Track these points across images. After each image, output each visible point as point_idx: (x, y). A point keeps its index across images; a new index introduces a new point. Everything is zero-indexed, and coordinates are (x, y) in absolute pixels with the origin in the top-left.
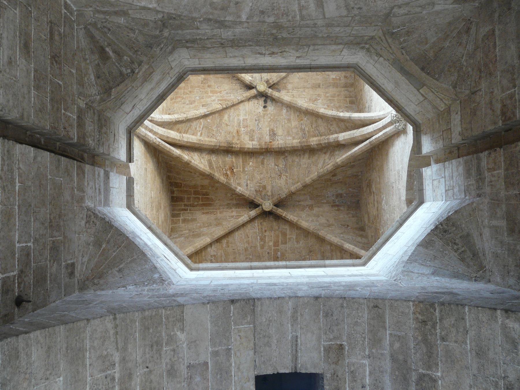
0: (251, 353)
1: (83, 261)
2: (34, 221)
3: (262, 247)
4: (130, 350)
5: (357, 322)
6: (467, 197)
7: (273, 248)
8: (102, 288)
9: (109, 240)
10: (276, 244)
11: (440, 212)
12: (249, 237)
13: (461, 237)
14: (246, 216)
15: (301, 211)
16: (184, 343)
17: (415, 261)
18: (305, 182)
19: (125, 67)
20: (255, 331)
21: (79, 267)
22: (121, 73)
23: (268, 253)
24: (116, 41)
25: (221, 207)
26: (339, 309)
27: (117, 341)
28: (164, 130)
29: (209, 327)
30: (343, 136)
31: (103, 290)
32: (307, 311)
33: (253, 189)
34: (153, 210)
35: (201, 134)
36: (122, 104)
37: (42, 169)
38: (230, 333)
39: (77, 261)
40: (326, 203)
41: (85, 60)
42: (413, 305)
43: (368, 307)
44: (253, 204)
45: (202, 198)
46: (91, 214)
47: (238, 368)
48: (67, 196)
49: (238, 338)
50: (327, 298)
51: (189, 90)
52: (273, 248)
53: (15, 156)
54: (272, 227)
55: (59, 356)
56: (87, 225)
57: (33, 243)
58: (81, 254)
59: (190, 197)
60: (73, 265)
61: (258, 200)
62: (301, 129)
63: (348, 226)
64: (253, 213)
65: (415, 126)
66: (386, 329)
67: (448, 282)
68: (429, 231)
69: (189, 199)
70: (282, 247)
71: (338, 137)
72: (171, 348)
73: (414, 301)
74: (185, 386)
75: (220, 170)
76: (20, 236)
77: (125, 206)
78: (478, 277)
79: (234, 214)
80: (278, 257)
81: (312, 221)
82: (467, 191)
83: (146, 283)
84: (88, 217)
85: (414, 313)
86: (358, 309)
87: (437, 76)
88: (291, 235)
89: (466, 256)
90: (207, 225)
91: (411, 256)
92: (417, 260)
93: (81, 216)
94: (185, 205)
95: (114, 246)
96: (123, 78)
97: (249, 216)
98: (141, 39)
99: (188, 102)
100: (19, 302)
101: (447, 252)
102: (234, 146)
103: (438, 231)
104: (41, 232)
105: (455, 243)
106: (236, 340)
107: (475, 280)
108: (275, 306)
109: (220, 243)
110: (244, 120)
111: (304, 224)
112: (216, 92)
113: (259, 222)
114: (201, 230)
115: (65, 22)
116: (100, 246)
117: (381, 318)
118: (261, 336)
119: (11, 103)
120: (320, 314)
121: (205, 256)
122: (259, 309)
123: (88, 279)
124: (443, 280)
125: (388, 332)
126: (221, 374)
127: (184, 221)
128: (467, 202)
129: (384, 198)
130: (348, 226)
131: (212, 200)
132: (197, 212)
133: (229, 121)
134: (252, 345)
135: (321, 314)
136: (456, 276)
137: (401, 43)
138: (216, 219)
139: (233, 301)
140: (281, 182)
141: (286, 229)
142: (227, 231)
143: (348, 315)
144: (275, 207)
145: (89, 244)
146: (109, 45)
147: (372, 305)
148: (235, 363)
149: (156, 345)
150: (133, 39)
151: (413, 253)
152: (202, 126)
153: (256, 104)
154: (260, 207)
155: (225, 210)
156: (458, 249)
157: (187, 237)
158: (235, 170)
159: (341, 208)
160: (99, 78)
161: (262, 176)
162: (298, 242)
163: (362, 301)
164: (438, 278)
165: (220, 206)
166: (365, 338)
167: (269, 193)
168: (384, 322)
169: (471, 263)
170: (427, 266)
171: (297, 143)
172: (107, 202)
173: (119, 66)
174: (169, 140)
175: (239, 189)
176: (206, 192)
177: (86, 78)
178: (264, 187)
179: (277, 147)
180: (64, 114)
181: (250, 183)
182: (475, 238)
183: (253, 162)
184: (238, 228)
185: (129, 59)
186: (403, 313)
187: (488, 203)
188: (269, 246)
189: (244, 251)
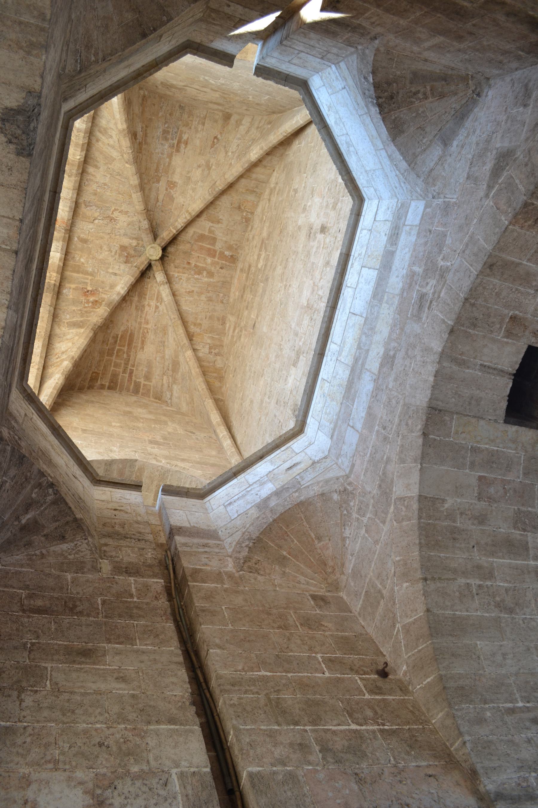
0: (482, 422)
1: (304, 582)
2: (291, 651)
3: (211, 274)
4: (456, 565)
5: (497, 292)
6: (360, 47)
7: (216, 259)
8: (340, 564)
9: (276, 545)
10: (212, 253)
11: (351, 82)
12: (193, 291)
13: (411, 83)
14: (161, 288)
15: (173, 201)
16: (456, 501)
17: (415, 156)
18: (135, 186)
19: (45, 496)
20: (462, 414)
21: (312, 588)
22: (54, 503)
23: (221, 268)
24: (13, 508)
25: (139, 320)
26: (474, 309)
27: (447, 579)
29: (446, 468)
31: (343, 565)
32: (460, 347)
33: (123, 266)
34: (138, 427)
36: (81, 499)
37: (228, 638)
38: (456, 444)
39: (306, 591)
40: (171, 160)
41: (43, 556)
42: (514, 225)
43: (488, 275)
44: (145, 273)
45: (120, 346)
46: (246, 565)
47: (493, 441)
48: (239, 600)
49: (463, 435)
50: (457, 319)
52: (216, 259)
53: (234, 676)
54: (185, 253)
55: (459, 645)
56: (262, 573)
57: (316, 653)
58: (297, 585)
59: (115, 362)
60: (314, 597)
63: (216, 138)
64: (159, 276)
65: (188, 50)
66: (521, 264)
67: (468, 135)
68: (379, 116)
69: (117, 365)
70: (218, 246)
72: (458, 516)
73: (510, 223)
74: (496, 505)
75: (86, 312)
76: (316, 670)
77: (200, 501)
78: (476, 89)
79: (153, 303)
80: (232, 256)
81: (194, 190)
82: (349, 43)
83: (345, 512)
84: (251, 570)
85: (522, 227)
86: (484, 288)
87: (165, 18)
88: (203, 226)
89: (440, 90)
90: (162, 348)
91: (404, 158)
92: (414, 154)
93: (253, 581)
94: (124, 372)
95: (285, 540)
96: (60, 501)
97: (164, 284)
98: (13, 472)
100: (384, 674)
101: (421, 110)
102: (53, 282)
103: (386, 106)
104: (299, 642)
105: (415, 94)
106: (464, 439)
107: (479, 95)
108: (443, 383)
109: (193, 336)
111: (197, 206)
113: (173, 269)
114: (167, 357)
115: (6, 586)
116: (285, 558)
117: (506, 265)
118: (468, 407)
119: (174, 680)
120: (470, 333)
121: (209, 362)
122: (440, 403)
123: (326, 579)
124: (461, 137)
125: (525, 263)
126: (493, 463)
127: (148, 377)
128: (370, 55)
129: (207, 78)
130: (216, 138)
131: (126, 331)
132: (138, 357)
134: (473, 420)
135: (470, 331)
136: (461, 116)
137: (97, 62)
138: (155, 333)
139: (425, 435)
140: (122, 220)
141: (194, 232)
142: (179, 322)
143: (486, 301)
144: (158, 241)
145: (284, 572)
146: (18, 518)
147: (488, 270)
148: (486, 444)
149: (455, 534)
150: (12, 483)
151: (402, 154)
154: (153, 263)
155: (144, 316)
156: (425, 94)
157: (175, 381)
158: (89, 288)
159: (185, 137)
160: (64, 537)
161: (105, 247)
162: (219, 222)
163: (478, 281)
164: (455, 143)
165: (136, 321)
166: (517, 289)
167: (134, 243)
168: (513, 262)
169: (453, 88)
170: (429, 146)
171: (70, 181)
172: (210, 534)
173: (44, 506)
175: (121, 288)
176: (113, 337)
177: (69, 557)
178: (123, 248)
179: (67, 214)
180: (138, 598)
181: (113, 268)
182: (425, 68)
183: (81, 257)
184: (177, 303)
185: (36, 490)
186: (515, 239)
187: (396, 37)
188: (213, 264)
189: (211, 303)
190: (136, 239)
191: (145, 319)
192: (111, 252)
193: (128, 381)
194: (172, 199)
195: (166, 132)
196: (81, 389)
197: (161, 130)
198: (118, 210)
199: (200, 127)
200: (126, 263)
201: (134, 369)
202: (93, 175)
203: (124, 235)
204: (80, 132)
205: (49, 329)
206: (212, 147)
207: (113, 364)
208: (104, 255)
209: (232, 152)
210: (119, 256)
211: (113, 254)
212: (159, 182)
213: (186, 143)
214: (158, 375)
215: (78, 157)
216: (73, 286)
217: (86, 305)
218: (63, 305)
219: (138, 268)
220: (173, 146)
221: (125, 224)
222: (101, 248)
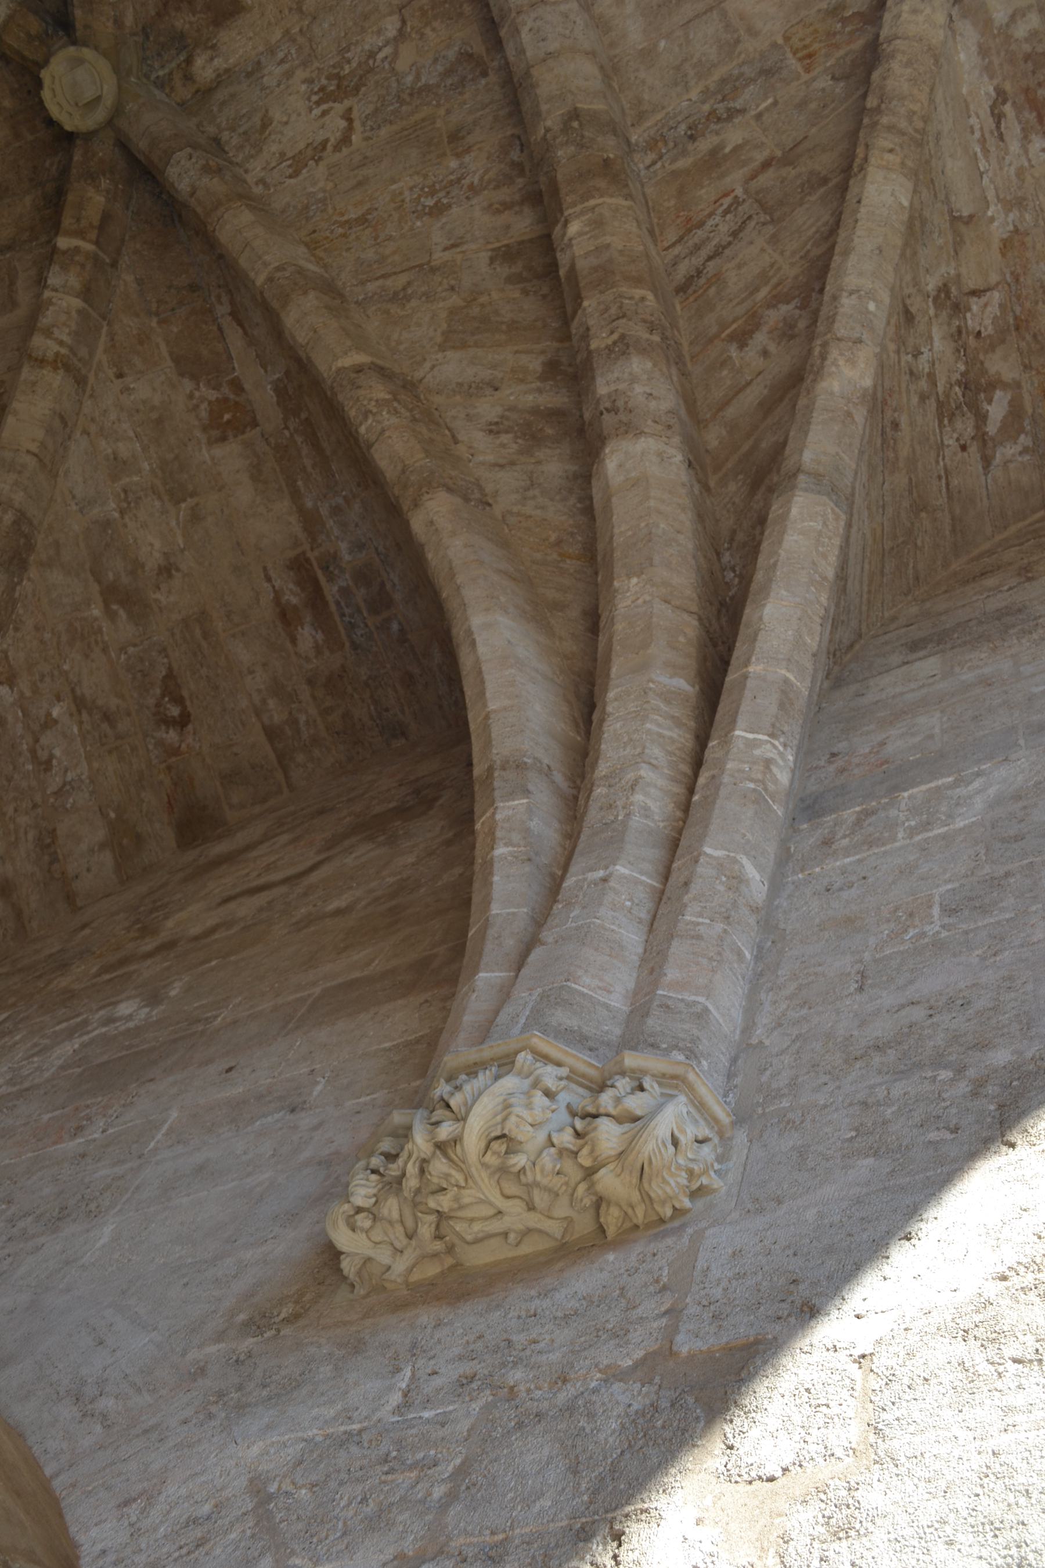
15: (177, 360)
30: (647, 474)
40: (301, 510)
62: (730, 87)
63: (183, 721)
71: (629, 429)
81: (119, 466)
130: (183, 721)
141: (14, 304)
144: (104, 150)
159: (307, 636)
167: (204, 68)
190: (208, 91)
194: (189, 366)
195: (381, 602)
197: (397, 597)
198: (337, 148)
199: (276, 714)
202: (506, 206)
204: (609, 349)
206: (170, 675)
209: (49, 723)
212: (276, 390)
213: (286, 617)
215: (574, 228)
220: (325, 569)
221: (277, 115)
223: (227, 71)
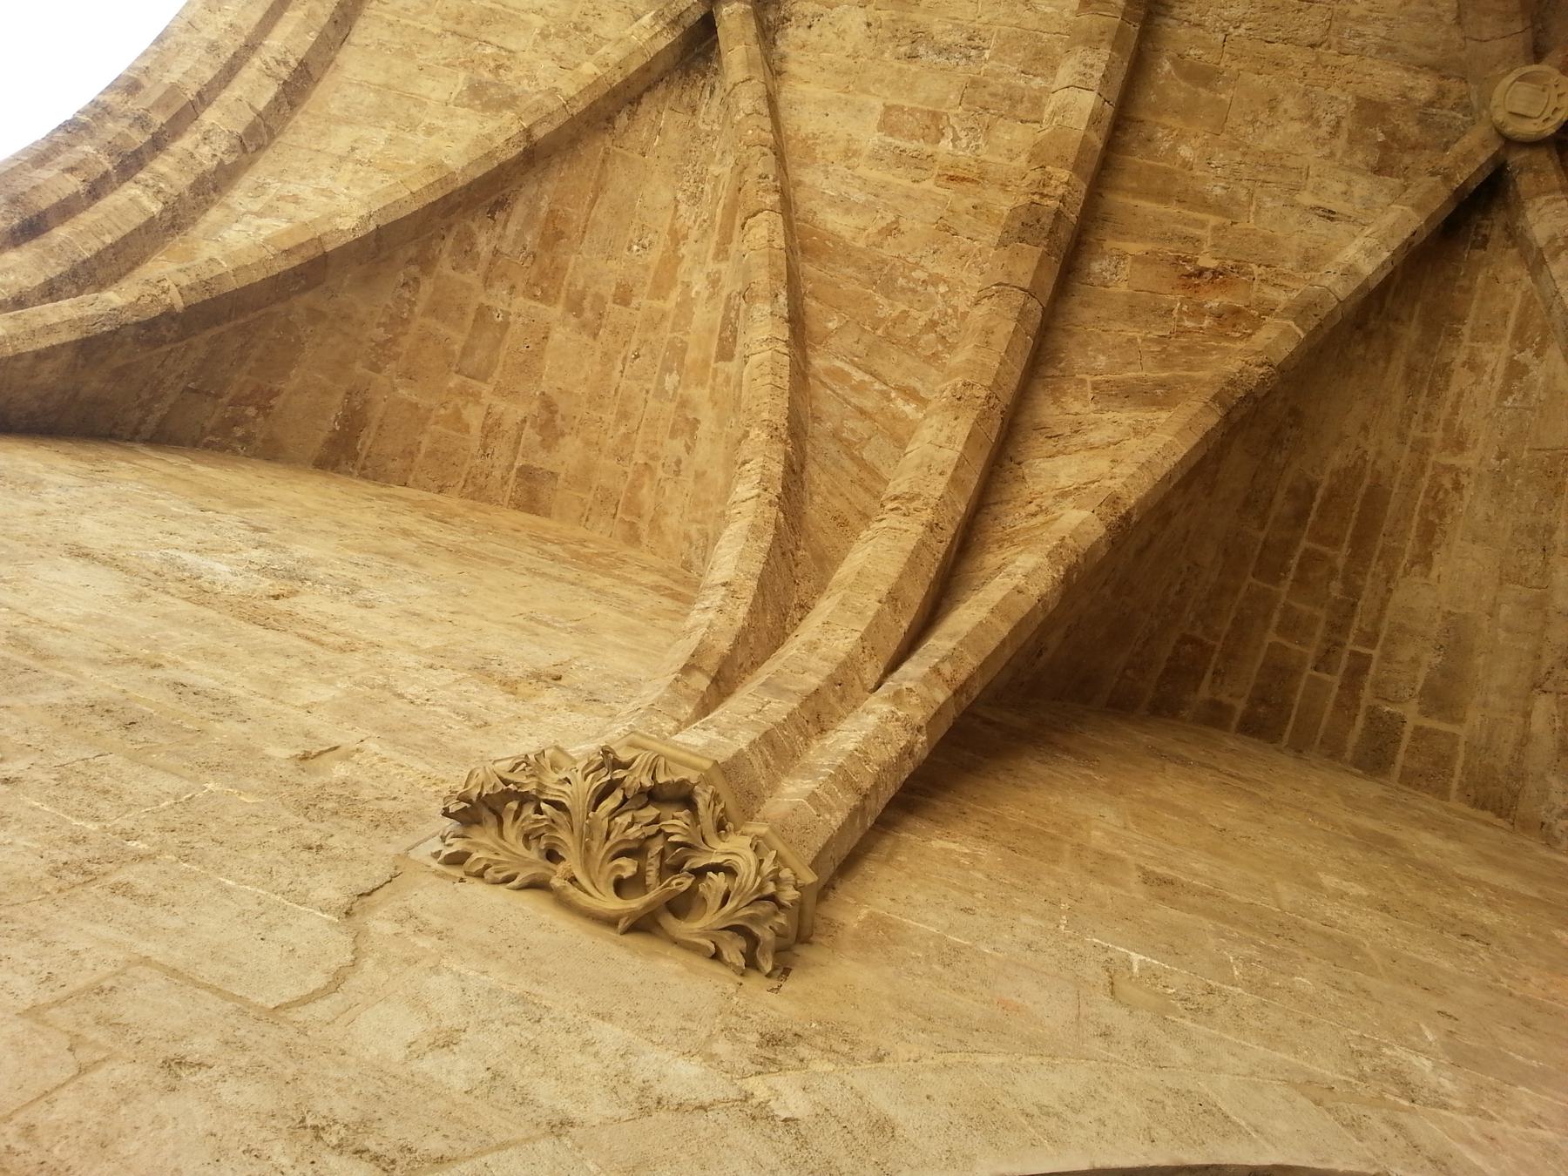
25: (1415, 432)
28: (825, 607)
33: (1363, 186)
35: (910, 394)
51: (610, 418)
59: (1288, 609)
61: (1469, 154)
69: (1293, 626)
90: (1536, 560)
94: (1324, 662)
99: (678, 445)
102: (1053, 204)
110: (886, 126)
112: (671, 261)
127: (1442, 696)
132: (1398, 597)
133: (866, 207)
152: (858, 376)
153: (812, 36)
154: (1516, 158)
155: (1442, 414)
158: (1207, 261)
161: (1289, 104)
165: (1402, 437)
167: (1424, 88)
174: (916, 595)
175: (1360, 250)
176: (1293, 492)
178: (1370, 110)
181: (1316, 191)
183: (1181, 138)
190: (1433, 68)
191: (1448, 427)
192: (1317, 124)
193: (1339, 705)
196: (1122, 706)
200: (1377, 171)
201: (1376, 653)
203: (1381, 50)
205: (1013, 384)
207: (1276, 618)
208: (1285, 133)
210: (1351, 141)
211: (1323, 131)
214: (1503, 691)
216: (1135, 248)
217: (1188, 324)
218: (1083, 315)
219: (1447, 178)
222: (1272, 104)
223: (1408, 70)
